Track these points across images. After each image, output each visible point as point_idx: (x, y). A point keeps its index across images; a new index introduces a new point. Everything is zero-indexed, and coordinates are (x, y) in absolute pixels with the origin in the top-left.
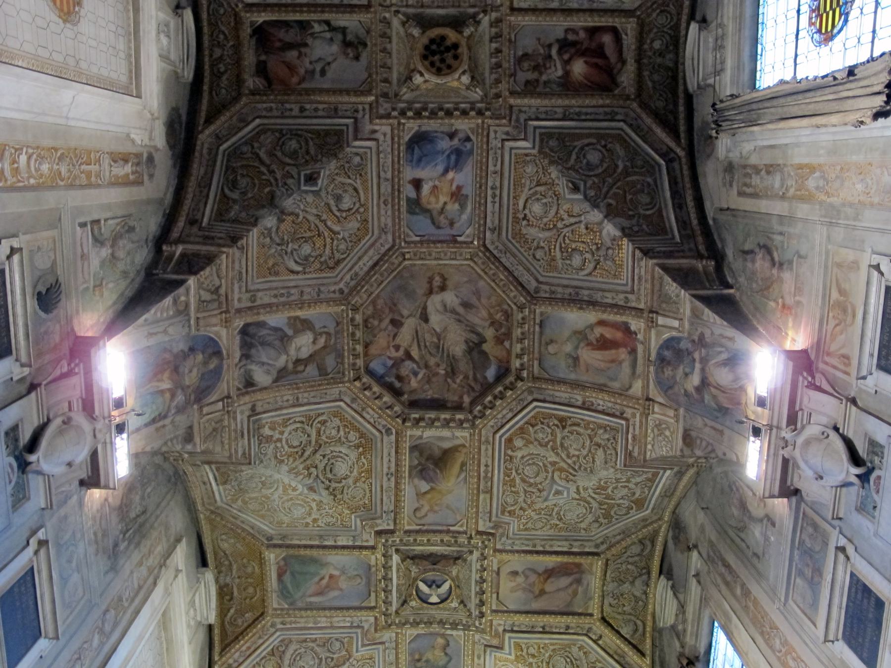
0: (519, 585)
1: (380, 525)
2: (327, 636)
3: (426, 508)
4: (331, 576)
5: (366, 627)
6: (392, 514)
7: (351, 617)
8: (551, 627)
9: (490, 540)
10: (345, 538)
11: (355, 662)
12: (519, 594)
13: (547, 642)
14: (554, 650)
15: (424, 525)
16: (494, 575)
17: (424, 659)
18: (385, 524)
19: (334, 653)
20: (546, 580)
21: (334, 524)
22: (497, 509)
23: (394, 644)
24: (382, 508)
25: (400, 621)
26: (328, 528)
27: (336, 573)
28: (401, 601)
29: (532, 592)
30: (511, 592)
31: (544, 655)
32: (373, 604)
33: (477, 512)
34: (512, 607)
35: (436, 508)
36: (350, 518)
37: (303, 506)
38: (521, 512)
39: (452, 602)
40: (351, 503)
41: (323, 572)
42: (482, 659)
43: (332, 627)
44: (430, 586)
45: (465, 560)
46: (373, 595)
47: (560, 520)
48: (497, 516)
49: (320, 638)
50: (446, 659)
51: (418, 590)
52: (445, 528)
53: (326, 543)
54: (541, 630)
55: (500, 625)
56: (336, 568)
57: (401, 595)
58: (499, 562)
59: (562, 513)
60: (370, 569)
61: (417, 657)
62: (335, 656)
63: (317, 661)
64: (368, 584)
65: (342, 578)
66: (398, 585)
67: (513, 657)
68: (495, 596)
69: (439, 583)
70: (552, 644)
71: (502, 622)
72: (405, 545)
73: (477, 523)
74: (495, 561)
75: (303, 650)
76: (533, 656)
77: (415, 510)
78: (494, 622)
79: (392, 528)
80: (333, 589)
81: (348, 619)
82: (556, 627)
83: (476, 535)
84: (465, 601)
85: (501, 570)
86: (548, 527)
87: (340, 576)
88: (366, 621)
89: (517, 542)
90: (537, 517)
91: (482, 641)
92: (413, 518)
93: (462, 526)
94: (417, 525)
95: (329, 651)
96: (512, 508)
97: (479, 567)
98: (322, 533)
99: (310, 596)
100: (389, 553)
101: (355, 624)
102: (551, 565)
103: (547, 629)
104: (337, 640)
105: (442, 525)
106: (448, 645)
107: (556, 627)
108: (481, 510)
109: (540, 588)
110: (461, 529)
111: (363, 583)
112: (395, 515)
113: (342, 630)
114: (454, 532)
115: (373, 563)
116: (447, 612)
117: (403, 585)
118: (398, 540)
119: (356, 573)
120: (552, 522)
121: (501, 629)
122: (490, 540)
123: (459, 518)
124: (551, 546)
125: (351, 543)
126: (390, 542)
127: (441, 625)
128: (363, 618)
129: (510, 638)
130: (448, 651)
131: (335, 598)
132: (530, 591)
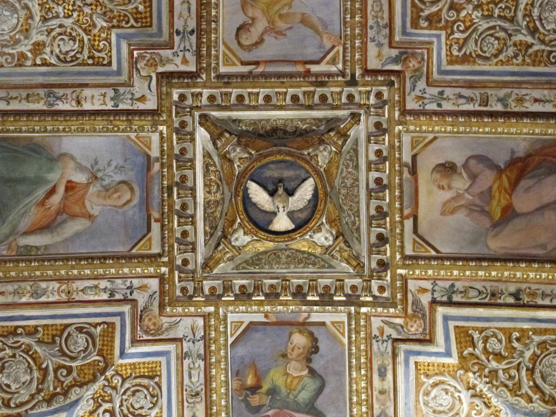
0: (458, 196)
1: (169, 61)
2: (58, 322)
3: (261, 25)
4: (70, 187)
5: (141, 304)
6: (193, 38)
7: (111, 279)
8: (533, 294)
9: (391, 84)
10: (96, 92)
11: (117, 381)
12: (461, 216)
13: (526, 326)
14: (542, 345)
15: (257, 63)
16: (406, 174)
17: (266, 387)
18: (178, 60)
19: (73, 359)
20: (514, 185)
21: (74, 58)
22: (404, 15)
23: (200, 346)
24: (172, 25)
25: (213, 289)
26: (68, 68)
27: (80, 178)
28: (213, 242)
29: (488, 214)
30: (443, 213)
31: (521, 354)
32: (156, 249)
33: (364, 25)
34: (445, 250)
35: (281, 25)
36: (108, 39)
37: (15, 11)
38: (453, 13)
39: (319, 230)
40: (110, 6)
41: (53, 177)
42: (390, 376)
43: (70, 303)
44: (272, 194)
45: (345, 136)
46: (156, 227)
47: (533, 32)
48: (404, 32)
49: (45, 326)
50: (312, 385)
51: (246, 199)
52: (300, 68)
53: (61, 106)
54: (511, 300)
55: (423, 290)
56: (81, 168)
57: (214, 228)
58: (414, 144)
59: (536, 13)
60: (149, 169)
61: (250, 381)
62: (74, 364)
63: (36, 374)
64: (146, 203)
65: (92, 189)
66: (207, 204)
67: (453, 360)
68: (409, 224)
69: (291, 185)
70: (536, 332)
71: (427, 285)
72: (221, 108)
73: (364, 50)
74: (406, 139)
75: (8, 351)
76: (499, 357)
77: (239, 29)
78: (412, 285)
79: (192, 68)
80: (73, 216)
81: (103, 284)
82: (544, 295)
83: (363, 75)
84: (347, 234)
85: (419, 164)
86: (510, 52)
87: (88, 185)
88: (143, 288)
89: (449, 92)
90: (484, 25)
91: (389, 331)
92: (234, 46)
93: (333, 62)
94: (243, 63)
95: (64, 354)
96: (434, 9)
97: (372, 157)
98: (53, 80)
99: (27, 233)
100: (189, 129)
101: (118, 297)
102: (521, 150)
103: (526, 299)
104: (80, 330)
105: (296, 63)
106: (315, 349)
107: (544, 295)
108: (370, 22)
109: (504, 203)
110: (333, 69)
111: (136, 201)
112: (199, 38)
113: (91, 310)
114: (317, 75)
115: (155, 153)
116: (311, 269)
117: (217, 203)
118: (206, 92)
119: (118, 178)
120: (519, 38)
121: (425, 299)
122: (391, 84)
123: (328, 45)
124: (520, 100)
125: (109, 106)
126: (189, 102)
127: (298, 300)
128: (136, 282)
129: (446, 318)
130: (318, 363)
131: (78, 235)
132: (483, 212)
